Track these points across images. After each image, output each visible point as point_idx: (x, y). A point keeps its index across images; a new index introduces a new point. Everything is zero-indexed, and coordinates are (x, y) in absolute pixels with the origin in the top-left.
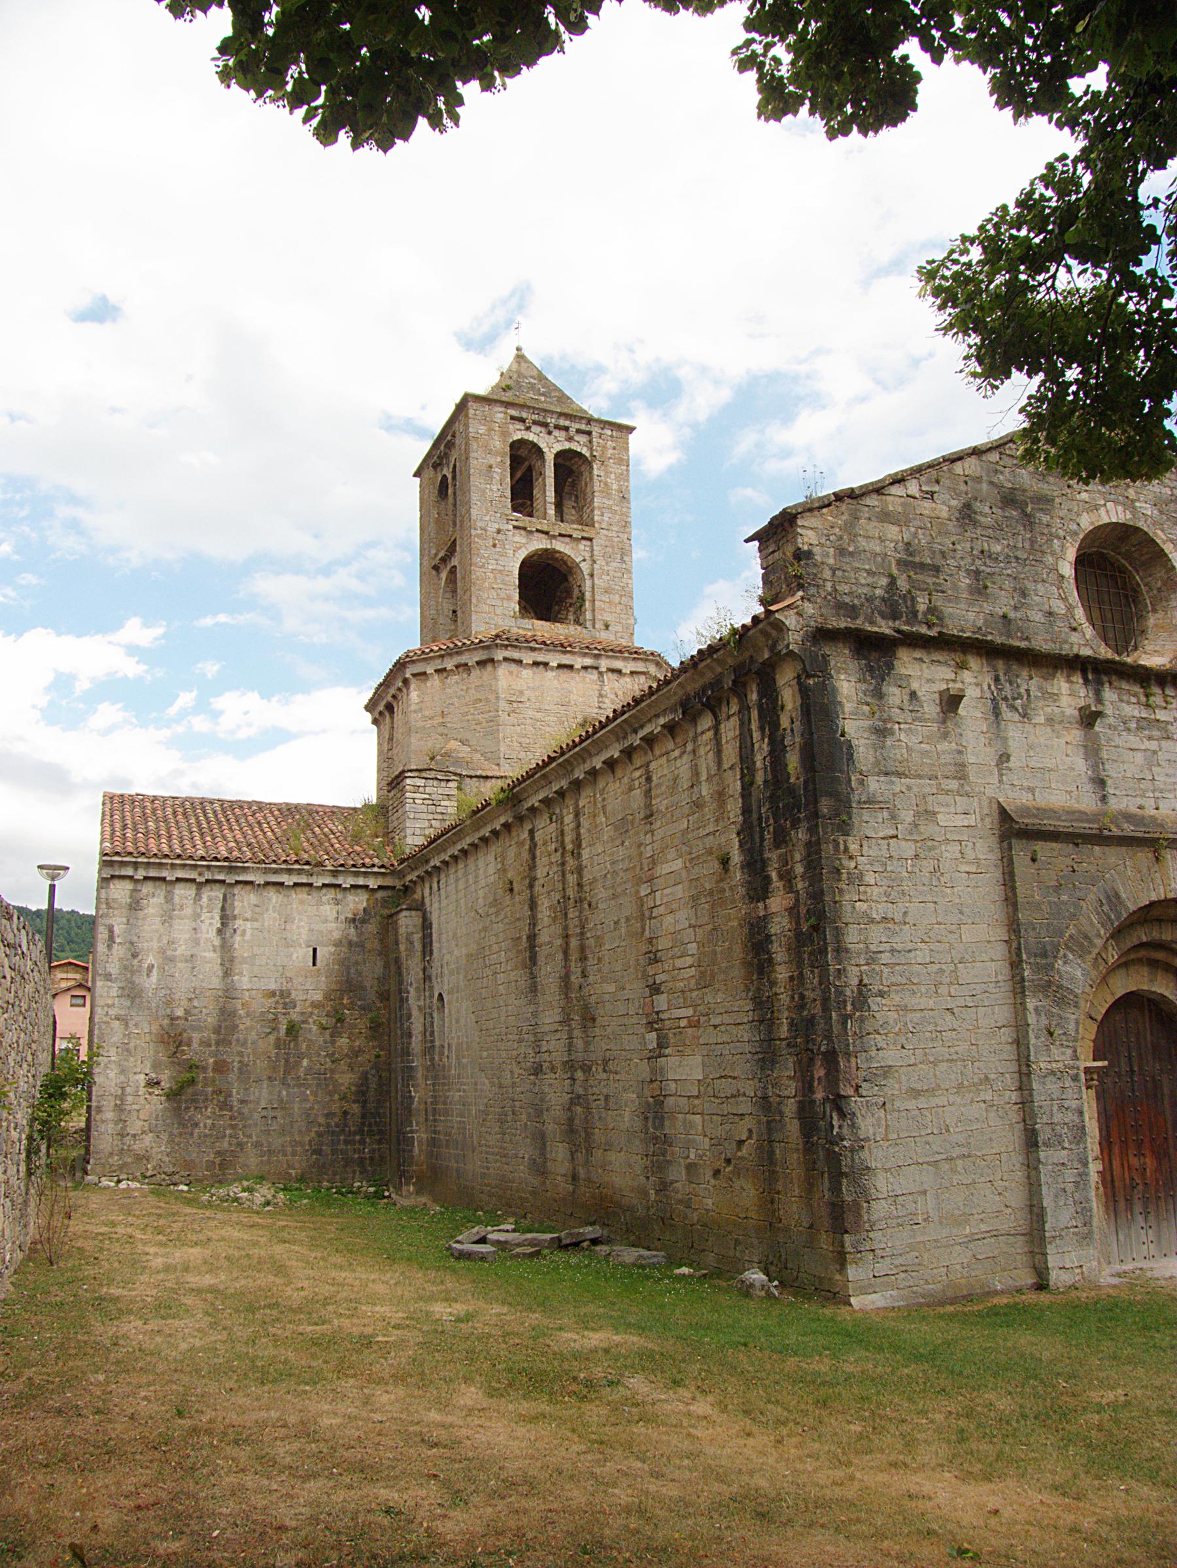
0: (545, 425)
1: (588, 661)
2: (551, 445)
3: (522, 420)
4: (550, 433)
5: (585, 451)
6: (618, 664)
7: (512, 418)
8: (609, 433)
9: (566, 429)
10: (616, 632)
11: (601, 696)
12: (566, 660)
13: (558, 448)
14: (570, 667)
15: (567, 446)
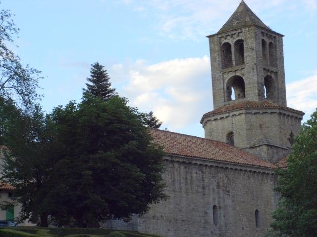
0: (229, 35)
1: (227, 115)
2: (232, 41)
3: (223, 37)
4: (232, 37)
5: (243, 39)
6: (235, 113)
7: (220, 38)
8: (247, 29)
9: (235, 34)
10: (252, 97)
11: (232, 124)
12: (221, 116)
13: (235, 41)
14: (223, 118)
15: (237, 39)
